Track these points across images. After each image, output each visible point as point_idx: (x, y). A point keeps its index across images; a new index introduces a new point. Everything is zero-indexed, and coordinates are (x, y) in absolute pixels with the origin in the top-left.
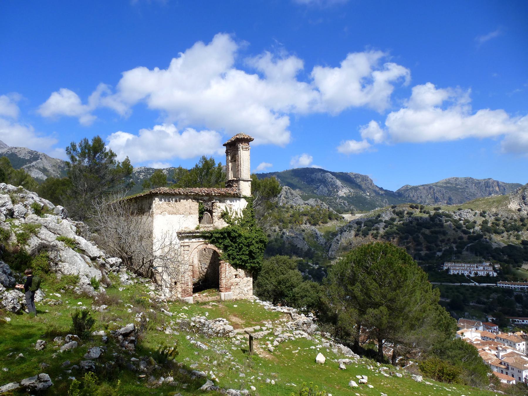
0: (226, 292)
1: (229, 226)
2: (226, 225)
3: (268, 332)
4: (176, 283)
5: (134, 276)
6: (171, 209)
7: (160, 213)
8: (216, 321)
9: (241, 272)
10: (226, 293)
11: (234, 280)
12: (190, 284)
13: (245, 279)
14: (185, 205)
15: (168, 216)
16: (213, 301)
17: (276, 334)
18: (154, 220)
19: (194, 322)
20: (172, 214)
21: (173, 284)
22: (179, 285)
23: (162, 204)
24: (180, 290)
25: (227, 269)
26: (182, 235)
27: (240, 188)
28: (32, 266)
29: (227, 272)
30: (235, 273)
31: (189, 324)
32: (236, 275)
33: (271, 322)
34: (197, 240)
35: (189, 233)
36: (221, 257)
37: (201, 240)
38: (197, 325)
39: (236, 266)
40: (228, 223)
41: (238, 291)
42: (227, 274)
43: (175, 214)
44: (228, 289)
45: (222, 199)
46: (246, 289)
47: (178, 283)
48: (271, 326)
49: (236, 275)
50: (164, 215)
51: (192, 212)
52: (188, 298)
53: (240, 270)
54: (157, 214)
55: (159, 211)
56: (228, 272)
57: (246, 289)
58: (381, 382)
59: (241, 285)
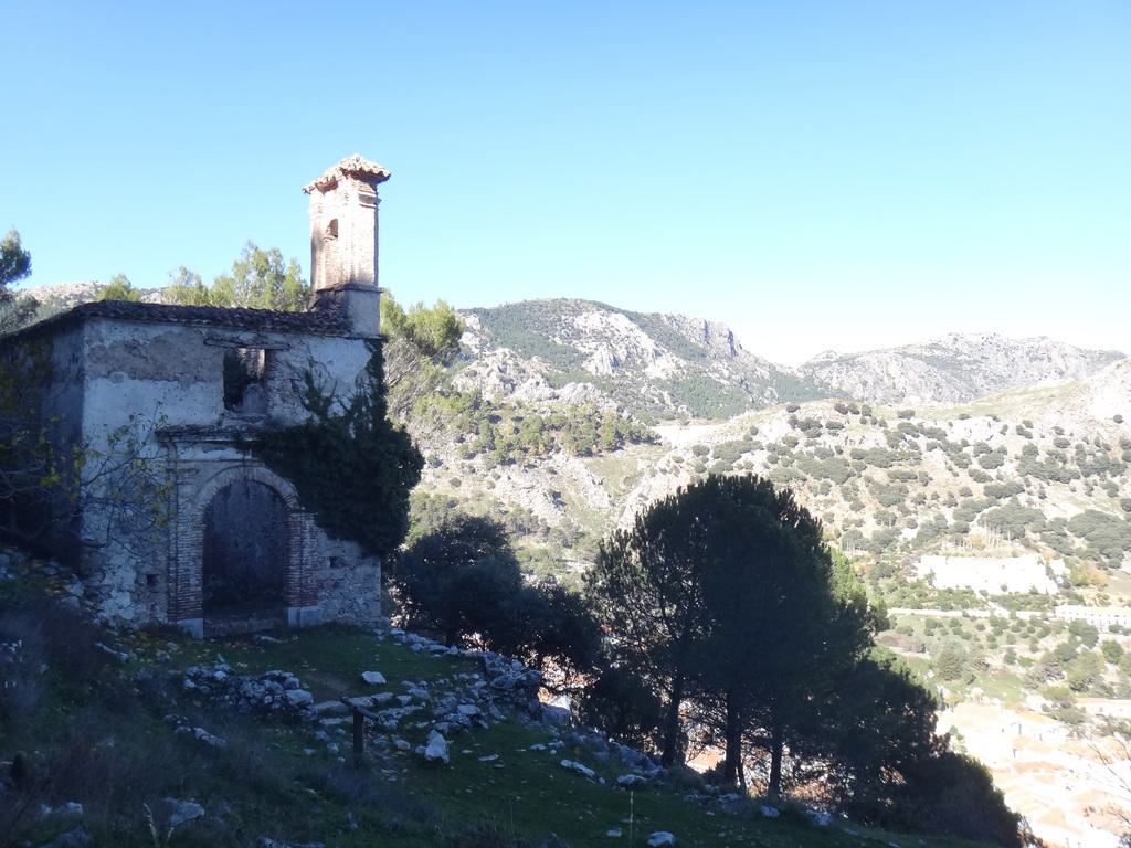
0: (302, 605)
1: (311, 419)
2: (303, 416)
3: (413, 708)
4: (151, 579)
5: (20, 557)
6: (139, 363)
7: (103, 373)
8: (265, 678)
9: (349, 550)
10: (303, 610)
11: (326, 572)
12: (193, 581)
13: (364, 570)
14: (183, 354)
15: (129, 385)
16: (267, 632)
17: (437, 712)
18: (86, 394)
19: (195, 678)
20: (141, 379)
21: (144, 581)
22: (161, 584)
23: (112, 347)
24: (163, 598)
25: (308, 540)
27: (350, 313)
29: (307, 550)
30: (329, 554)
31: (177, 682)
32: (333, 560)
33: (425, 683)
34: (217, 454)
36: (292, 503)
37: (231, 453)
38: (204, 688)
39: (334, 532)
40: (308, 408)
42: (306, 554)
43: (153, 378)
44: (307, 598)
45: (294, 342)
46: (361, 601)
48: (424, 693)
49: (333, 560)
51: (205, 373)
52: (188, 621)
53: (347, 545)
54: (96, 376)
57: (361, 601)
58: (719, 830)
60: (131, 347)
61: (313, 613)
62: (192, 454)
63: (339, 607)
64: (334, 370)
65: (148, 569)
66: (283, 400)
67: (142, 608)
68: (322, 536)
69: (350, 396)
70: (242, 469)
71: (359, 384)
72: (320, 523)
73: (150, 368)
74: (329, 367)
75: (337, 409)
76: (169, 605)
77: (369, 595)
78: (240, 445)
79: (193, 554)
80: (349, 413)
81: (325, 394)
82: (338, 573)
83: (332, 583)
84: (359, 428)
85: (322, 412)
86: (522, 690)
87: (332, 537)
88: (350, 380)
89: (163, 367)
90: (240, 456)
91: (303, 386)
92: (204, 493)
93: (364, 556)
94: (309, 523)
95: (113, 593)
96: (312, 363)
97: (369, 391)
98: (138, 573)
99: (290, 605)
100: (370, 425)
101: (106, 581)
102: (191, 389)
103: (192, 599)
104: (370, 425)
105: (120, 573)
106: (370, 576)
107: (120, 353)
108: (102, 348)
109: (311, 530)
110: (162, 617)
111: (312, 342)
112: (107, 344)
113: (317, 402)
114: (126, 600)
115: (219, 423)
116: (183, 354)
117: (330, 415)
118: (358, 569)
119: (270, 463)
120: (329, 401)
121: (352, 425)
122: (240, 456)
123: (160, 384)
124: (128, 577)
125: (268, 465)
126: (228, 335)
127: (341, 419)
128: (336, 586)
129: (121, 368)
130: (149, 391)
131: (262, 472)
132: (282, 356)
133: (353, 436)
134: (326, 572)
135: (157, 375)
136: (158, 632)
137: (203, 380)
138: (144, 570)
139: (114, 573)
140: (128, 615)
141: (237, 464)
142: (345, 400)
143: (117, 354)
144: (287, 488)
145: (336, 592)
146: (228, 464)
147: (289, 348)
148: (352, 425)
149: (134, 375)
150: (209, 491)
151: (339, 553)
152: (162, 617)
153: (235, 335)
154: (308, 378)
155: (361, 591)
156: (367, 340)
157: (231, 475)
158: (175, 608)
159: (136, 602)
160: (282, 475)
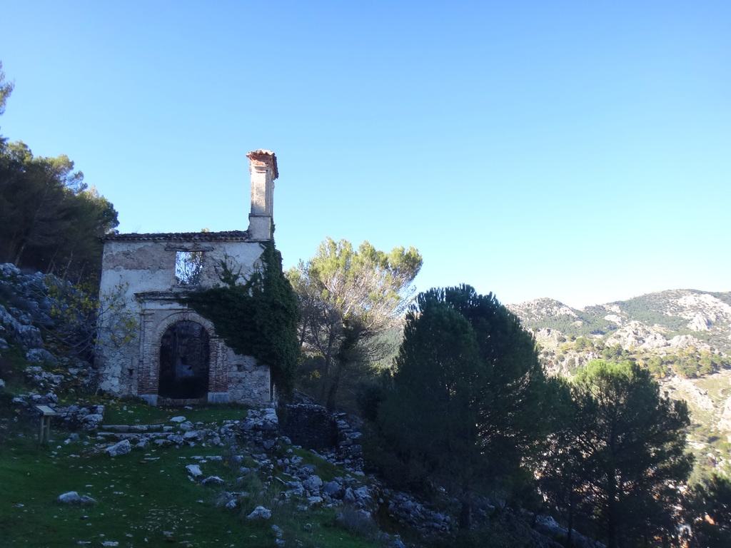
0: (217, 391)
4: (131, 371)
6: (129, 261)
9: (248, 361)
12: (151, 374)
13: (257, 373)
14: (153, 256)
15: (123, 272)
18: (102, 278)
20: (130, 269)
22: (135, 375)
23: (117, 255)
24: (135, 382)
25: (220, 354)
26: (141, 297)
28: (105, 386)
29: (220, 359)
30: (235, 363)
32: (239, 366)
35: (156, 300)
37: (176, 306)
41: (240, 392)
42: (219, 362)
43: (137, 269)
44: (224, 387)
45: (216, 246)
46: (256, 392)
47: (134, 371)
50: (119, 270)
52: (148, 395)
53: (247, 358)
55: (111, 265)
56: (224, 358)
57: (256, 392)
59: (247, 382)
60: (126, 254)
61: (227, 396)
62: (151, 306)
63: (241, 394)
64: (240, 260)
65: (128, 366)
66: (209, 277)
67: (124, 387)
68: (231, 352)
69: (250, 273)
70: (182, 314)
71: (255, 266)
72: (228, 344)
73: (135, 264)
74: (236, 259)
75: (241, 281)
76: (139, 386)
77: (262, 388)
78: (182, 302)
79: (152, 359)
80: (249, 284)
81: (234, 273)
82: (241, 374)
83: (238, 380)
84: (256, 292)
85: (232, 283)
86: (260, 432)
87: (237, 353)
88: (251, 264)
89: (142, 263)
90: (181, 307)
91: (221, 269)
92: (159, 327)
93: (258, 365)
94: (221, 344)
95: (109, 378)
96: (226, 257)
97: (262, 270)
98: (123, 368)
99: (210, 391)
100: (263, 289)
101: (106, 371)
102: (157, 273)
103: (151, 383)
104: (263, 289)
105: (113, 368)
106: (262, 377)
107: (121, 257)
108: (112, 255)
109: (223, 348)
110: (135, 392)
111: (226, 245)
112: (114, 253)
113: (228, 276)
114: (116, 382)
115: (171, 290)
116: (153, 256)
117: (237, 283)
118: (254, 373)
119: (200, 311)
120: (236, 277)
121: (250, 289)
122: (181, 307)
123: (140, 271)
124: (118, 370)
125: (198, 313)
126: (178, 245)
127: (243, 286)
128: (240, 382)
129: (121, 264)
130: (133, 275)
131: (194, 316)
132: (208, 254)
133: (252, 296)
134: (234, 373)
135: (139, 267)
136: (129, 400)
137: (164, 269)
138: (126, 366)
139: (110, 368)
140: (116, 390)
141: (177, 311)
142: (247, 276)
143: (119, 258)
144: (209, 324)
145: (240, 386)
146: (174, 312)
147: (212, 249)
148: (250, 289)
149: (127, 267)
150: (164, 325)
151: (241, 362)
152: (135, 392)
153: (182, 245)
154: (224, 265)
155: (256, 386)
156: (260, 242)
157: (176, 318)
158: (142, 388)
159: (121, 383)
160: (206, 317)
